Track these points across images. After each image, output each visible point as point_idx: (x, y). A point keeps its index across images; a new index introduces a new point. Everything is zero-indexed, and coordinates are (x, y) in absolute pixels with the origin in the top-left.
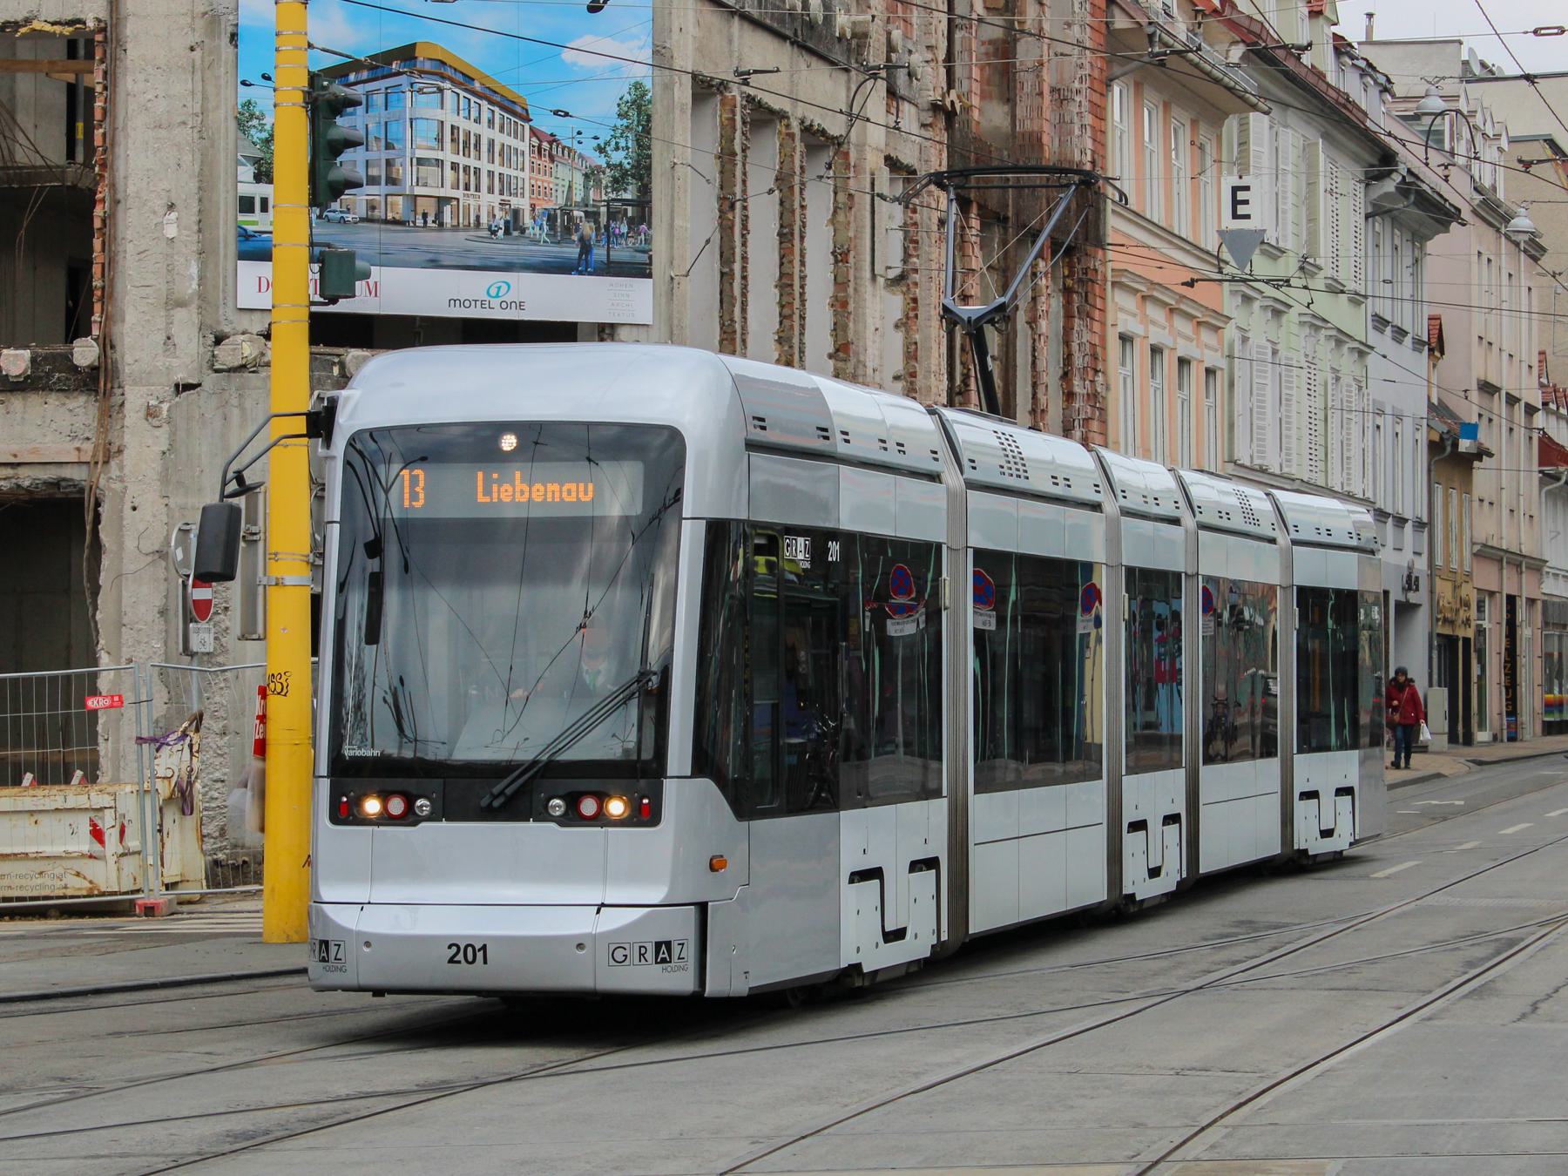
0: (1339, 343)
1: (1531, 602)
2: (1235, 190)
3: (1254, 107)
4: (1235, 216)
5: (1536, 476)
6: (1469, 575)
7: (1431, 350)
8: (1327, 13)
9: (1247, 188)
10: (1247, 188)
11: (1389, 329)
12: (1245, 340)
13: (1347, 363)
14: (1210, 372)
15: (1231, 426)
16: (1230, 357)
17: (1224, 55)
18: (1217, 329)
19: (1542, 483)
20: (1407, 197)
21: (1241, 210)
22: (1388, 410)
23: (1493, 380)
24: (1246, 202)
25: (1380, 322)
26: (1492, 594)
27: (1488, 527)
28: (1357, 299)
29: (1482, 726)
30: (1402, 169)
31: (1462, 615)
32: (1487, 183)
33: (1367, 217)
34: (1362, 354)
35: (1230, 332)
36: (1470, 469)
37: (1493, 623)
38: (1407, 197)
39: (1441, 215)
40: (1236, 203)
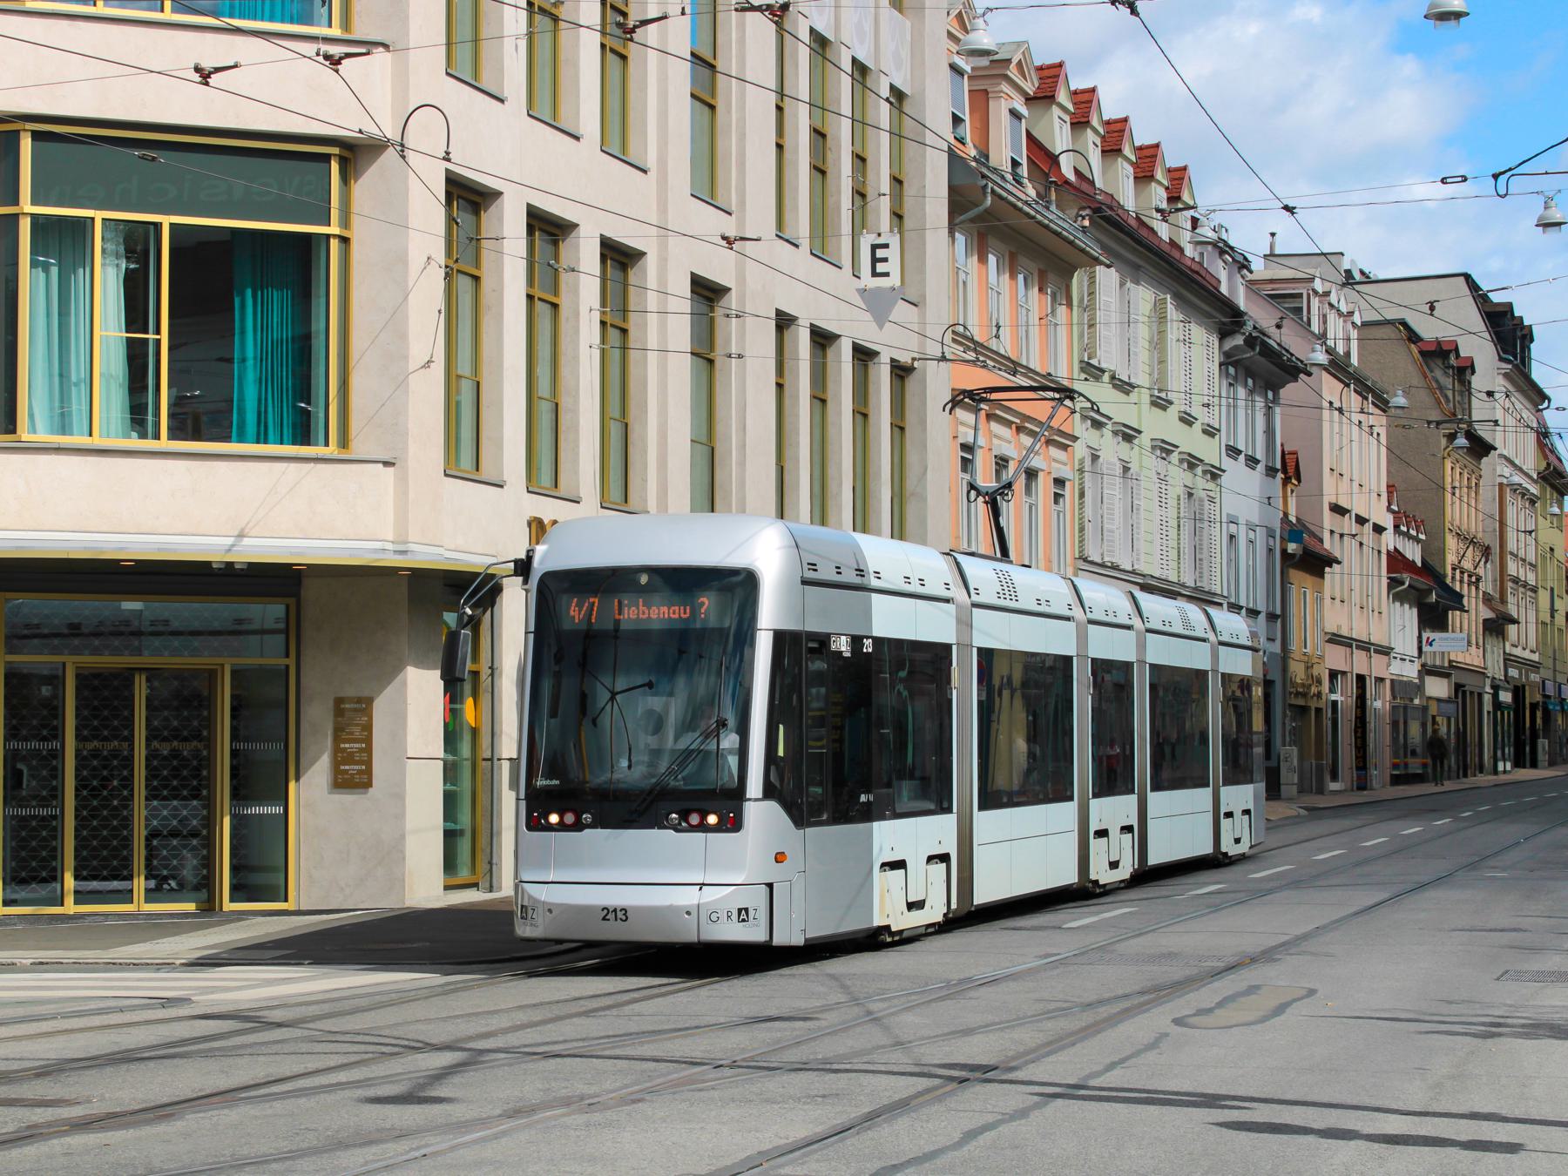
0: (1192, 466)
1: (1380, 680)
2: (874, 247)
3: (1097, 261)
4: (875, 274)
5: (1385, 581)
6: (1321, 657)
7: (1286, 481)
8: (1186, 197)
9: (886, 246)
10: (886, 246)
11: (1242, 458)
12: (1095, 458)
13: (1201, 483)
14: (1059, 482)
15: (1082, 529)
16: (1081, 471)
17: (1065, 221)
18: (1065, 447)
19: (1390, 588)
20: (1253, 349)
21: (880, 268)
22: (1242, 521)
23: (1344, 503)
24: (885, 260)
25: (1233, 451)
26: (1344, 673)
27: (1336, 619)
28: (1210, 432)
29: (1334, 777)
30: (1249, 328)
31: (1314, 690)
32: (1341, 350)
33: (1221, 365)
34: (1214, 477)
35: (1080, 450)
36: (1321, 575)
37: (1343, 697)
38: (1253, 349)
39: (1293, 370)
40: (875, 260)
